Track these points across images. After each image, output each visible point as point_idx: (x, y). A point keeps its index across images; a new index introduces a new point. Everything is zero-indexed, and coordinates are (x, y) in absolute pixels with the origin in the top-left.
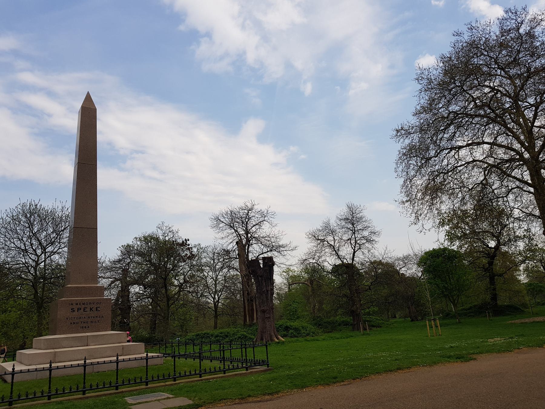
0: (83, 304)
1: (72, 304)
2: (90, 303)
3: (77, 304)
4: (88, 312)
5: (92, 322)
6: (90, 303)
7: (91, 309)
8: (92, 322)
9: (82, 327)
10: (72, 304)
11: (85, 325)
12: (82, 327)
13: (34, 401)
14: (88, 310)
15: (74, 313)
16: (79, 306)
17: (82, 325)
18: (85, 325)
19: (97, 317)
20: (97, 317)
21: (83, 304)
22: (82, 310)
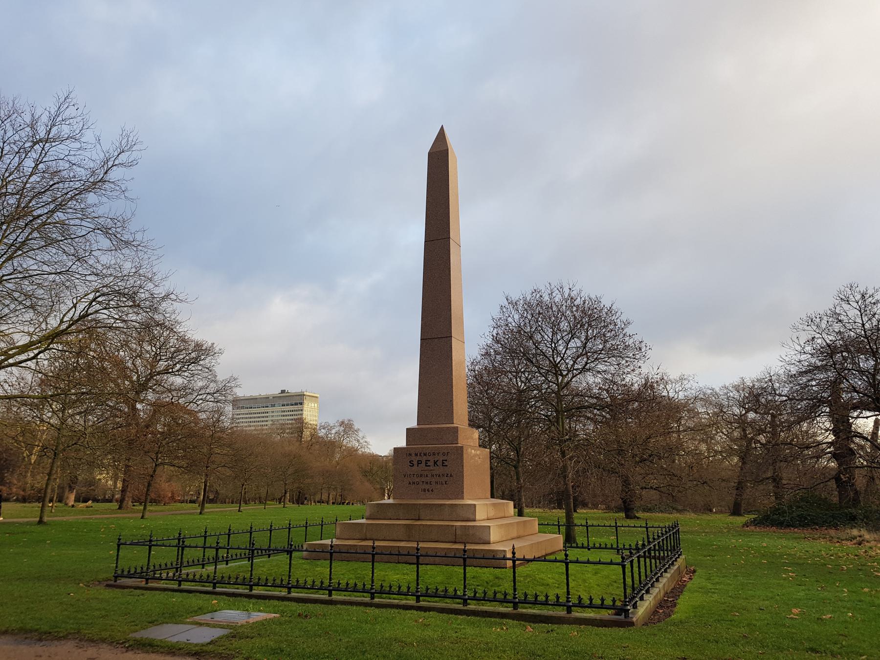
0: (425, 455)
1: (410, 455)
2: (434, 454)
3: (416, 455)
4: (431, 468)
5: (436, 483)
6: (434, 454)
7: (435, 463)
8: (436, 483)
9: (425, 490)
10: (410, 455)
11: (427, 487)
12: (425, 490)
13: (204, 586)
14: (431, 463)
15: (413, 468)
16: (418, 458)
17: (423, 487)
18: (427, 487)
19: (443, 475)
20: (443, 475)
21: (425, 455)
22: (424, 463)
